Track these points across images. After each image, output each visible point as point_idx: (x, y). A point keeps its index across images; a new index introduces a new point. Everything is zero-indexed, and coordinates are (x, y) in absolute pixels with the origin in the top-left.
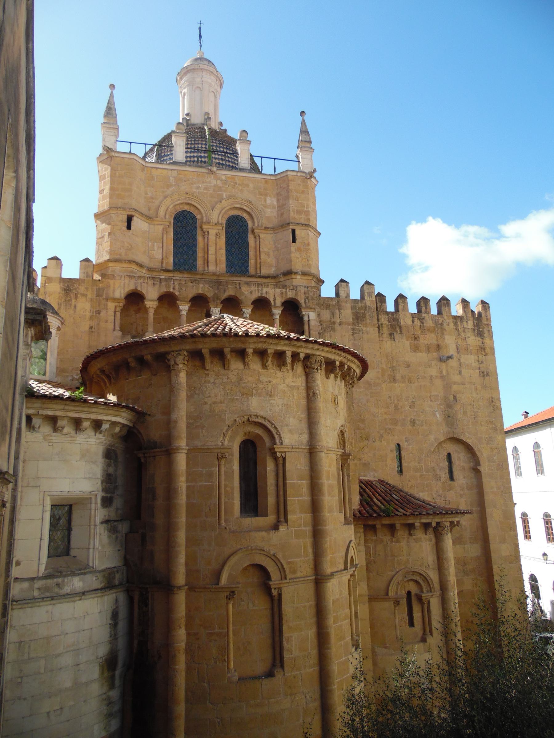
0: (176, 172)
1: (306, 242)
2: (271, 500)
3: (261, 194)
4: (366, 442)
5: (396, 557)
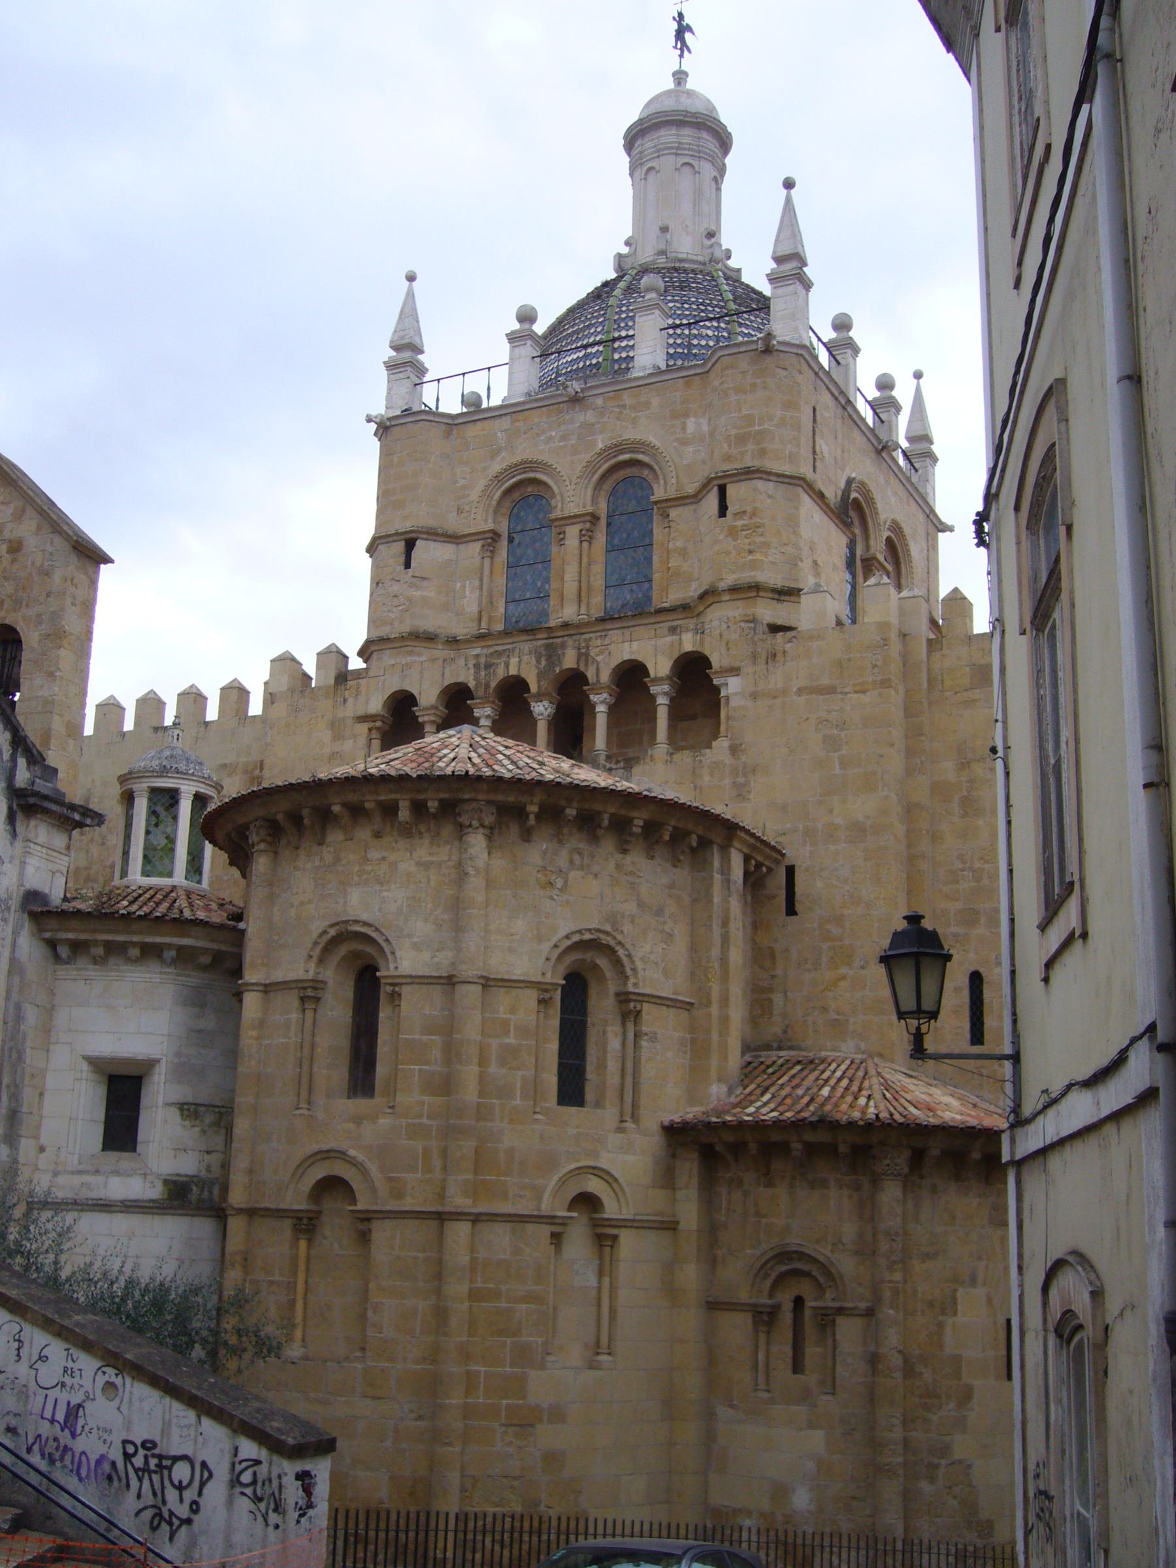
0: (508, 419)
1: (749, 509)
2: (382, 1070)
3: (675, 415)
4: (844, 970)
5: (764, 1216)
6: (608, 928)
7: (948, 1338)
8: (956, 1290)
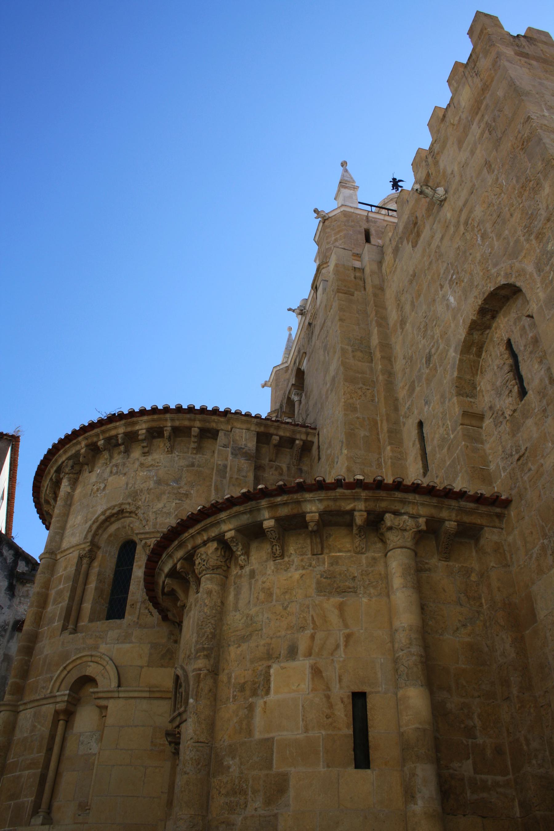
6: (130, 500)
7: (258, 720)
8: (269, 667)
